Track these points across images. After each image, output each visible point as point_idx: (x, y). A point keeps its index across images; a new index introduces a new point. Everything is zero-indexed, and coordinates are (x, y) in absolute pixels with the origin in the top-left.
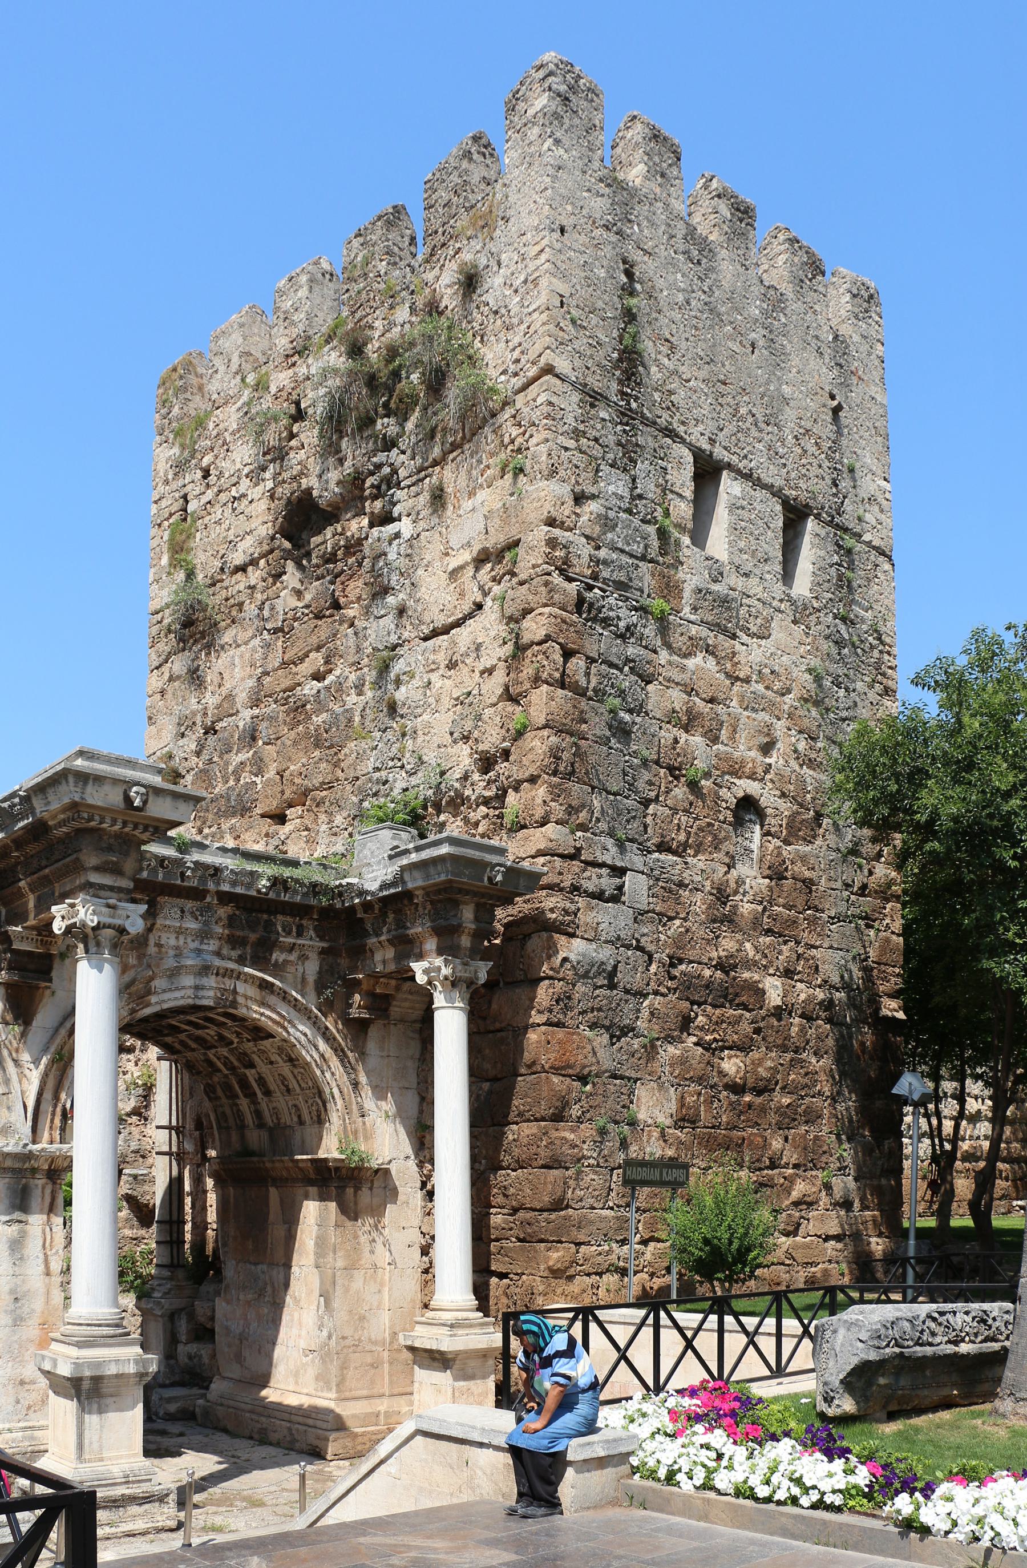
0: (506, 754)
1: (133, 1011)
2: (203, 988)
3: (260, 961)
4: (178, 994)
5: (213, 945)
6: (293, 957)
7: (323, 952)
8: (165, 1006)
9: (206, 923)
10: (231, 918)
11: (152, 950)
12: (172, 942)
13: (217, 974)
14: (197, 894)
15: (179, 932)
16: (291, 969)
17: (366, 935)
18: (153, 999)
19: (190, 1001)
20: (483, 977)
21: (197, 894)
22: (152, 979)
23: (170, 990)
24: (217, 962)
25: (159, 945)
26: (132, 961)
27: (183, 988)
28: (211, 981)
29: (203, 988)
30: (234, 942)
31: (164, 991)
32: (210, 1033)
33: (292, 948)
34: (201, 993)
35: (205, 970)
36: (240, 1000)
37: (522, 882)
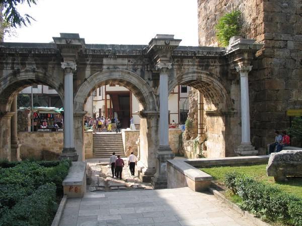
0: (257, 17)
1: (179, 83)
3: (206, 69)
5: (196, 67)
6: (214, 68)
7: (220, 66)
10: (199, 61)
11: (183, 69)
12: (187, 67)
14: (191, 57)
15: (188, 65)
16: (213, 70)
17: (228, 61)
20: (250, 69)
24: (196, 70)
25: (184, 68)
26: (179, 72)
28: (196, 75)
30: (200, 66)
32: (200, 85)
33: (213, 66)
35: (194, 72)
37: (257, 47)
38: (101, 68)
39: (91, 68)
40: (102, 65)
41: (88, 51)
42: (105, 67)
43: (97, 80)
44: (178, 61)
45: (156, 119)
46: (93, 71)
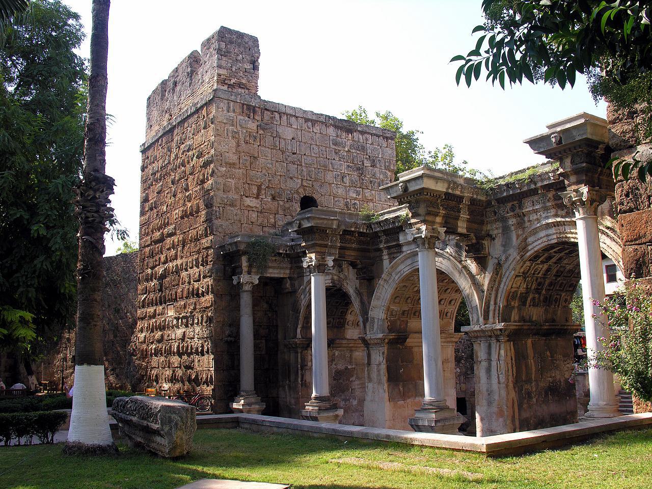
1: (522, 256)
2: (550, 235)
4: (539, 242)
8: (536, 249)
9: (544, 203)
11: (527, 224)
12: (535, 217)
13: (555, 226)
14: (534, 192)
15: (536, 211)
18: (530, 248)
19: (546, 243)
21: (534, 192)
22: (526, 239)
23: (536, 241)
25: (529, 221)
26: (520, 232)
27: (541, 238)
29: (550, 235)
31: (533, 242)
34: (550, 238)
36: (569, 235)
38: (401, 252)
39: (388, 254)
40: (399, 246)
41: (373, 226)
42: (404, 249)
43: (396, 275)
44: (513, 209)
45: (487, 344)
46: (391, 259)
